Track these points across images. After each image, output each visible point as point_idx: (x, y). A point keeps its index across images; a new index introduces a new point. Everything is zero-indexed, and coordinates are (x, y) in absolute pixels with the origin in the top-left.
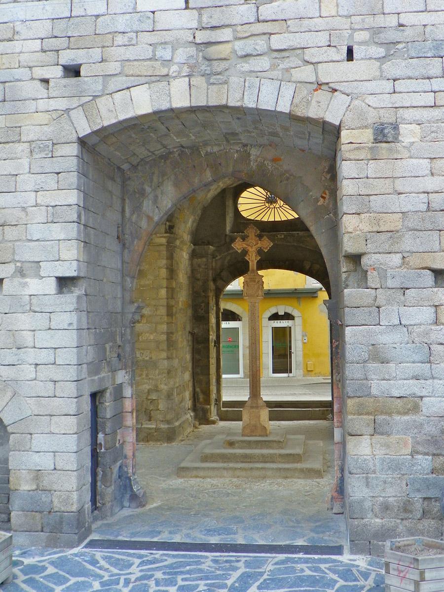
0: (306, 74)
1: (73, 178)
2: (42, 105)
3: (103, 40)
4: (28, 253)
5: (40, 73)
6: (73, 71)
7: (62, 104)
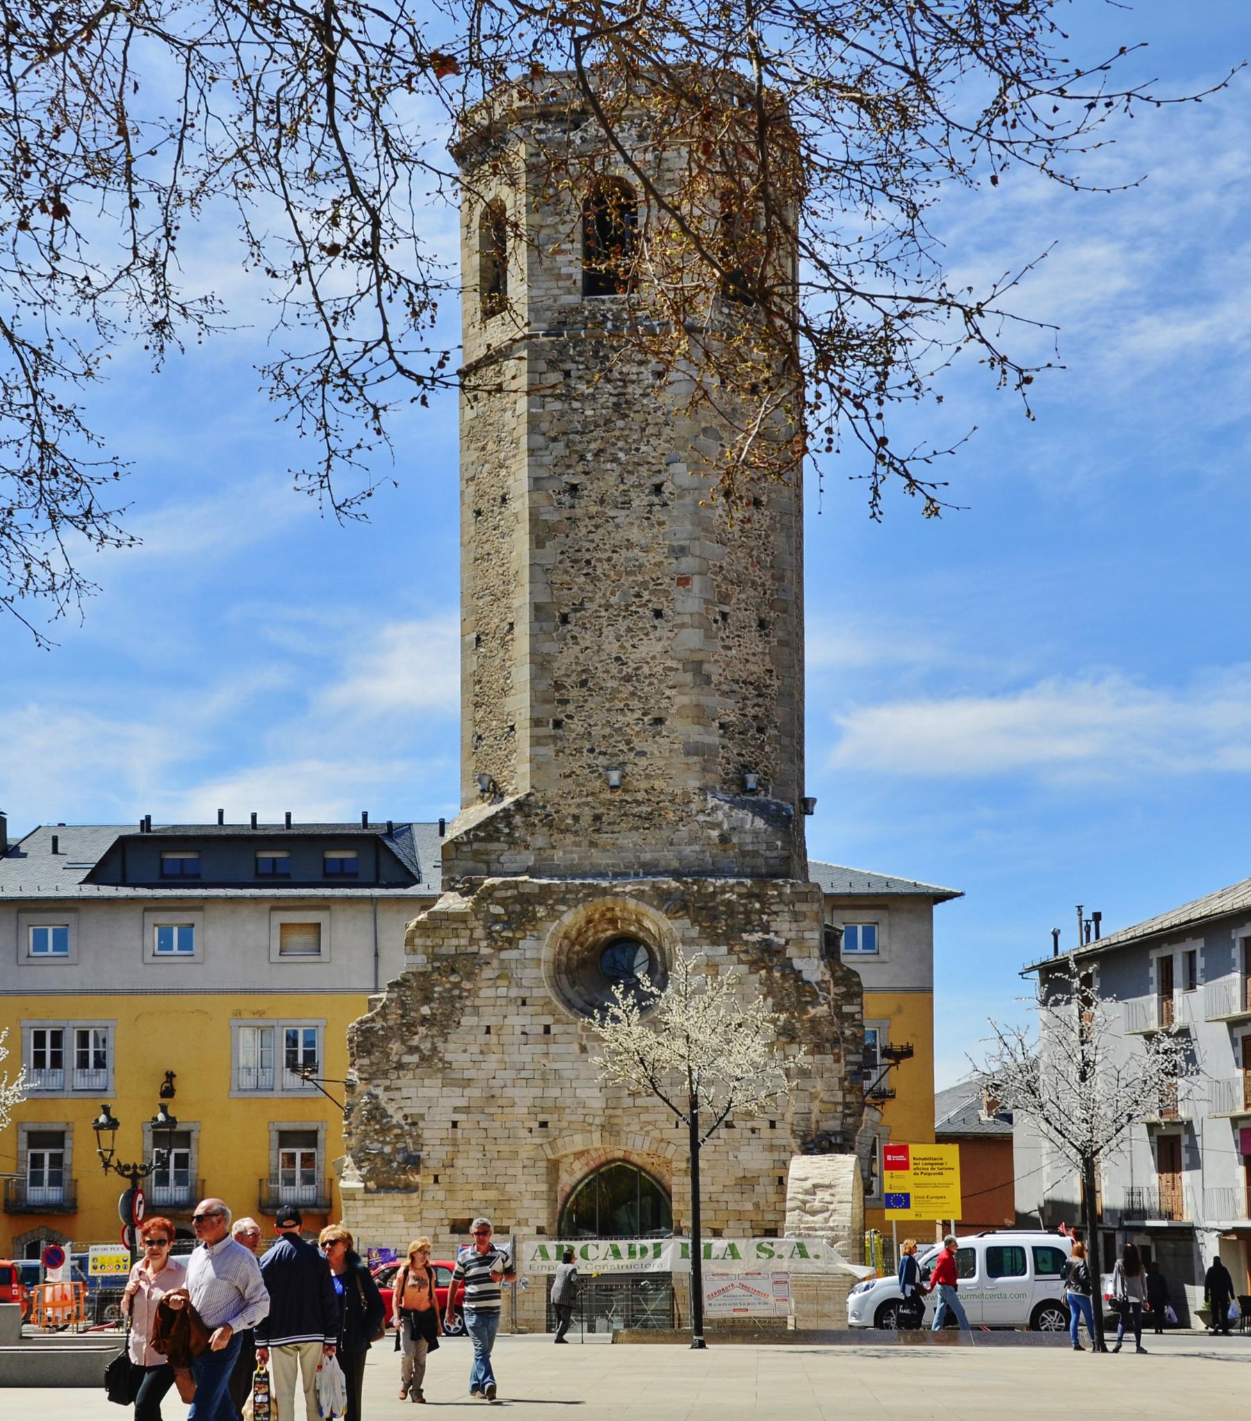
0: (656, 1134)
1: (544, 1178)
2: (529, 1141)
3: (558, 1109)
4: (521, 1215)
5: (528, 1124)
6: (544, 1125)
7: (539, 1141)
